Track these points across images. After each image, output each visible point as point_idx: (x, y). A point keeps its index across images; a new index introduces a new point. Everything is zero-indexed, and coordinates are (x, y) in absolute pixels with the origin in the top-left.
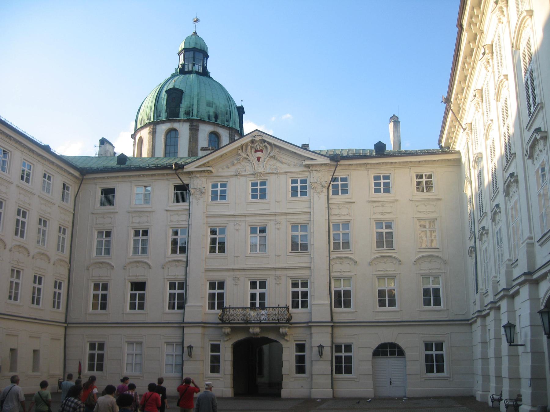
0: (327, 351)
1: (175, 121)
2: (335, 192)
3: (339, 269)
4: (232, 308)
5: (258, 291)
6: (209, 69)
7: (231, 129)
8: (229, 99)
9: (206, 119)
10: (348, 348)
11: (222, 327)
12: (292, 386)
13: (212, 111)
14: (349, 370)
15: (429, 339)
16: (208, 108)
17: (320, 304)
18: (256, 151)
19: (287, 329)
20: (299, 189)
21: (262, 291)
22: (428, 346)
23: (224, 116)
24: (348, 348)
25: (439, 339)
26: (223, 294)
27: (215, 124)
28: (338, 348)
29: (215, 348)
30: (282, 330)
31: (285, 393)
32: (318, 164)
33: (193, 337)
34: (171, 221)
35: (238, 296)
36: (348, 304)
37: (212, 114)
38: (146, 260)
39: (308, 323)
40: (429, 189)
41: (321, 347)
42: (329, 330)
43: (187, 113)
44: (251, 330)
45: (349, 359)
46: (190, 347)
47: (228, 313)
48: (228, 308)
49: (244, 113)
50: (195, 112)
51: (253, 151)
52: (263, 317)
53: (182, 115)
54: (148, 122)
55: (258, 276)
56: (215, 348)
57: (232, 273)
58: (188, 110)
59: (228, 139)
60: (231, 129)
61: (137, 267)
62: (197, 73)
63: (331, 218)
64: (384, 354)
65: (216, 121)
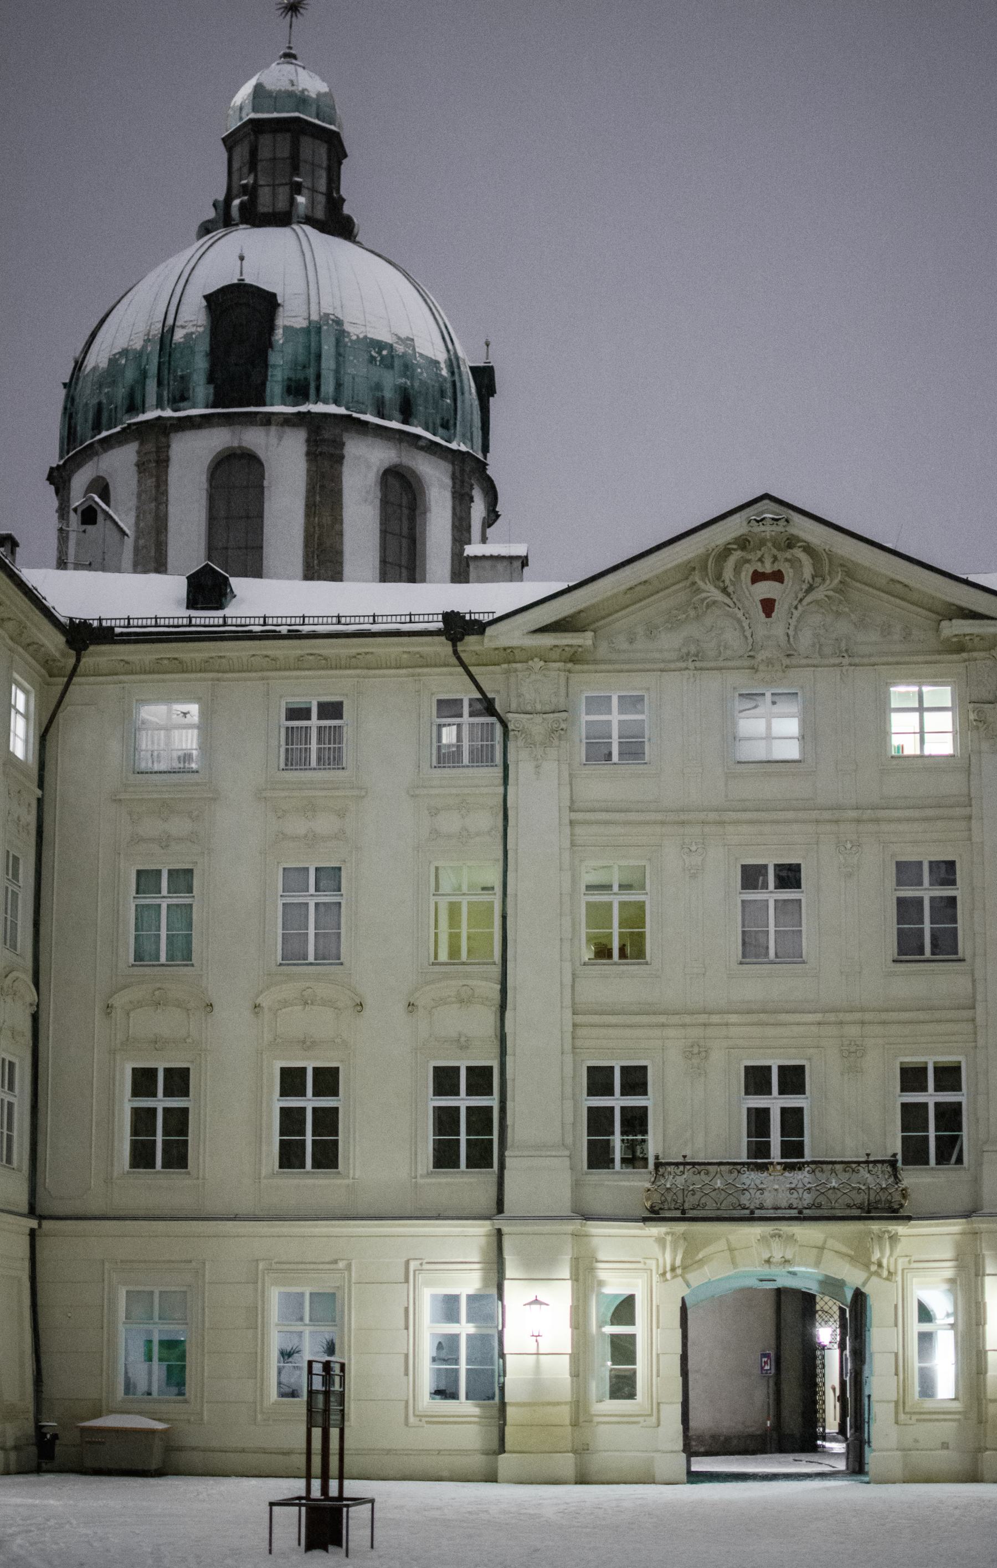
1: (251, 419)
5: (775, 1103)
6: (347, 210)
13: (390, 381)
16: (378, 373)
18: (757, 577)
21: (792, 1101)
23: (436, 404)
26: (185, 1111)
48: (677, 1164)
49: (492, 392)
50: (328, 386)
51: (746, 575)
58: (300, 375)
59: (448, 495)
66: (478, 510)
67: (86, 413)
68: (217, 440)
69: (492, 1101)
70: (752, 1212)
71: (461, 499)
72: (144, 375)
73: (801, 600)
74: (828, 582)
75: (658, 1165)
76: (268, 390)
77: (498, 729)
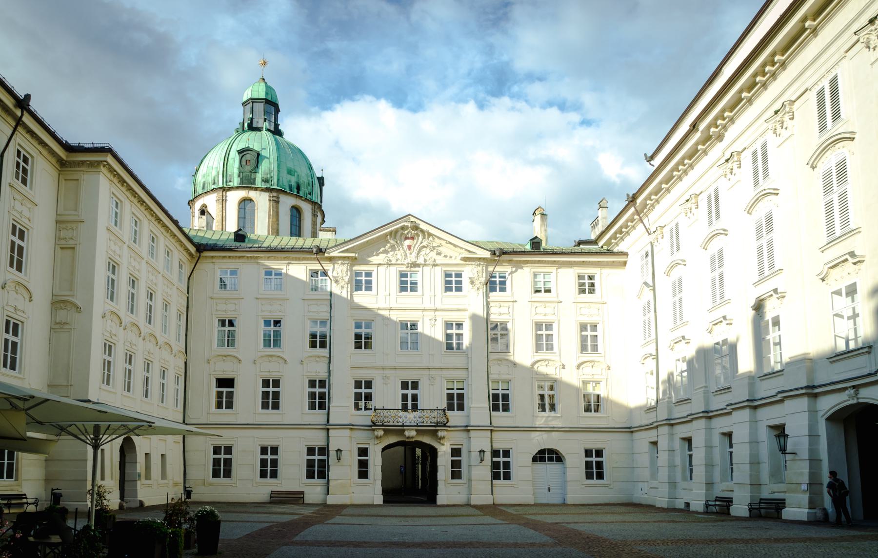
0: (488, 456)
3: (497, 372)
5: (410, 392)
7: (314, 203)
8: (310, 168)
10: (507, 453)
11: (374, 430)
12: (448, 491)
13: (293, 181)
14: (507, 476)
15: (589, 446)
18: (406, 238)
19: (446, 433)
20: (453, 283)
21: (415, 392)
22: (588, 453)
24: (507, 453)
25: (598, 446)
27: (298, 196)
28: (495, 453)
29: (363, 452)
30: (440, 434)
33: (340, 440)
34: (309, 312)
35: (387, 396)
36: (506, 408)
37: (293, 184)
38: (236, 354)
39: (467, 426)
40: (592, 291)
41: (482, 452)
43: (266, 181)
44: (407, 433)
45: (507, 465)
46: (339, 451)
49: (323, 185)
51: (403, 237)
52: (420, 420)
53: (259, 183)
54: (213, 187)
55: (410, 377)
56: (363, 452)
57: (381, 371)
60: (314, 203)
61: (270, 361)
62: (269, 130)
64: (542, 459)
65: (298, 192)
66: (319, 219)
69: (326, 390)
71: (314, 215)
75: (375, 410)
77: (329, 281)
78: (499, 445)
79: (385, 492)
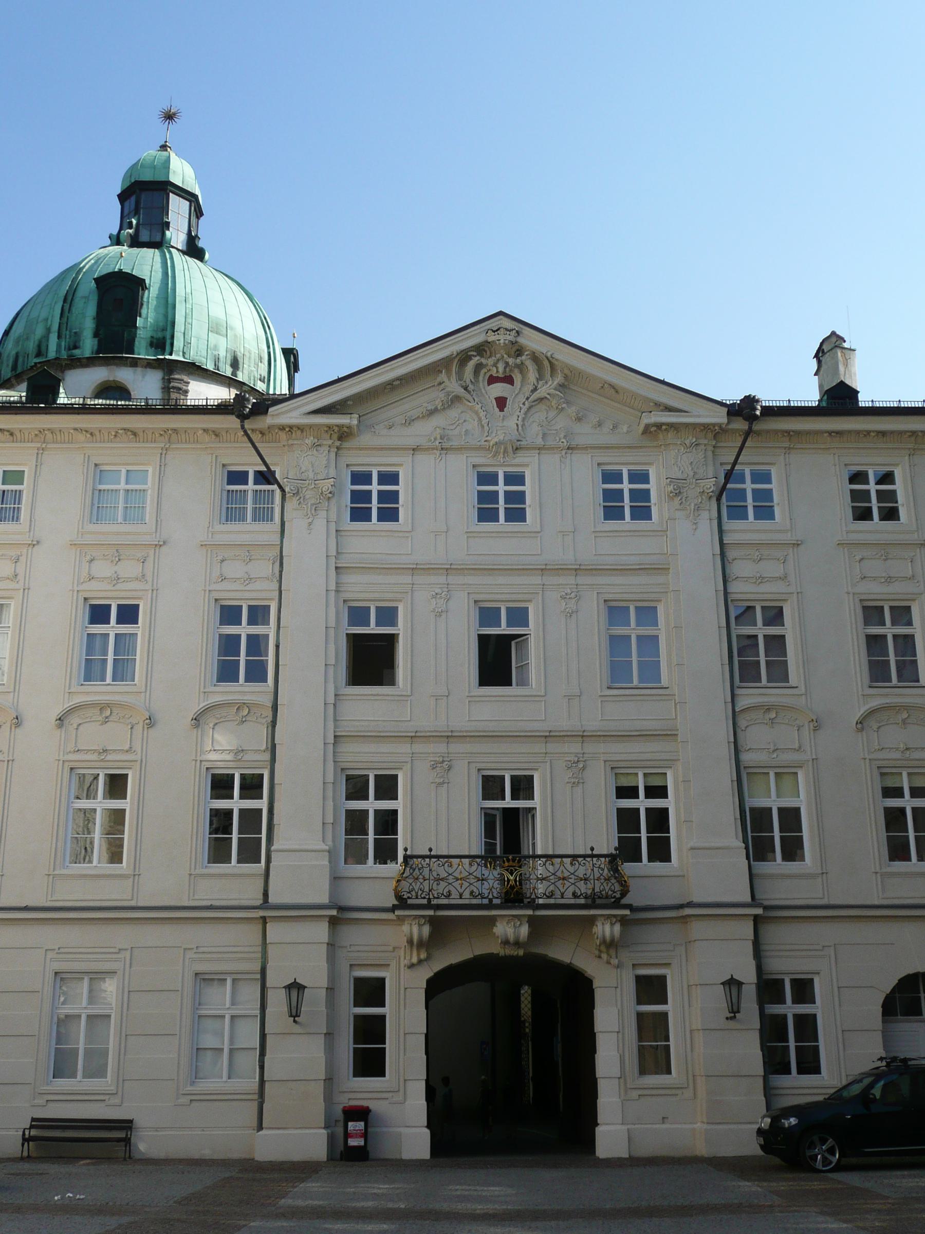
1: (124, 362)
2: (738, 513)
4: (438, 857)
9: (210, 367)
10: (804, 990)
17: (704, 853)
18: (492, 380)
20: (622, 501)
31: (610, 1138)
32: (687, 425)
37: (222, 353)
42: (748, 929)
47: (426, 872)
48: (423, 857)
49: (296, 369)
50: (178, 343)
53: (142, 352)
58: (160, 335)
63: (733, 587)
65: (234, 374)
67: (8, 360)
68: (99, 375)
69: (262, 804)
70: (491, 900)
72: (48, 331)
73: (528, 399)
74: (550, 383)
75: (406, 858)
76: (136, 343)
77: (278, 493)
78: (785, 965)
79: (438, 1118)
